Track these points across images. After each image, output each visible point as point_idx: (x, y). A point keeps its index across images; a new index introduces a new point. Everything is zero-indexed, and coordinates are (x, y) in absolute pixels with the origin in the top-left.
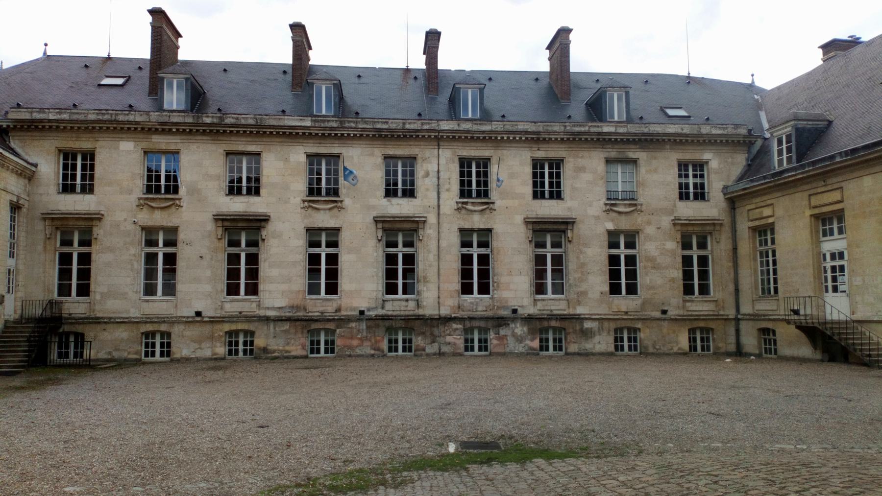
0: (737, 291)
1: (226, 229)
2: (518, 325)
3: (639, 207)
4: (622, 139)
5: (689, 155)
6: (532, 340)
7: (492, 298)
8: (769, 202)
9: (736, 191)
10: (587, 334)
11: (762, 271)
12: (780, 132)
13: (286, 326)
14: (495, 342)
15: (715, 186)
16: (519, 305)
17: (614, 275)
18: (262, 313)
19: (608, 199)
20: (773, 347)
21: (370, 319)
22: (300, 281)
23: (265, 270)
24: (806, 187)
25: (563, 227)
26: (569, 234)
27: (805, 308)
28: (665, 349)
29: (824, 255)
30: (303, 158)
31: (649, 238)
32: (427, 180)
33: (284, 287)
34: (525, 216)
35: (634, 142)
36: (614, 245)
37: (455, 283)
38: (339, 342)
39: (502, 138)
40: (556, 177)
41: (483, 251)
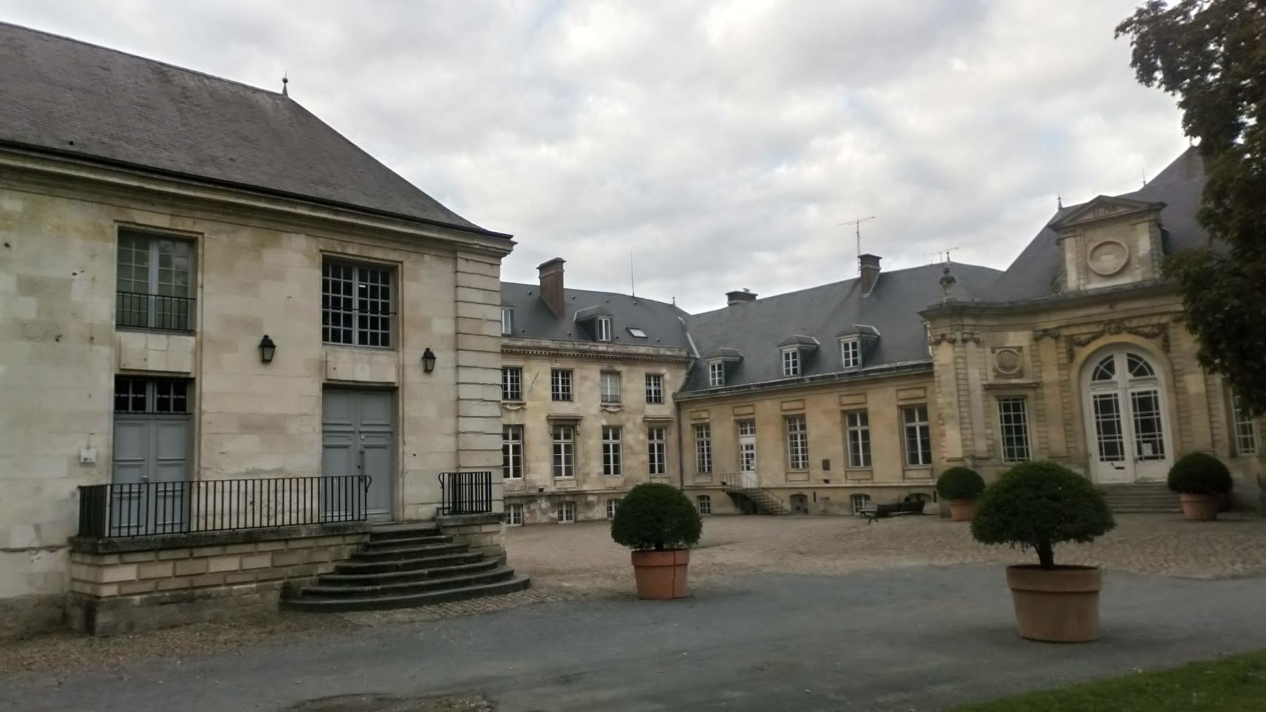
2: (543, 501)
3: (623, 408)
4: (612, 357)
5: (653, 370)
6: (553, 513)
7: (524, 480)
8: (707, 408)
9: (683, 398)
10: (590, 506)
11: (699, 456)
12: (714, 362)
14: (527, 515)
16: (544, 484)
17: (607, 459)
19: (602, 401)
20: (707, 508)
24: (731, 401)
25: (573, 423)
26: (578, 428)
27: (731, 481)
29: (742, 447)
34: (547, 415)
35: (619, 359)
36: (606, 437)
39: (533, 352)
40: (566, 382)
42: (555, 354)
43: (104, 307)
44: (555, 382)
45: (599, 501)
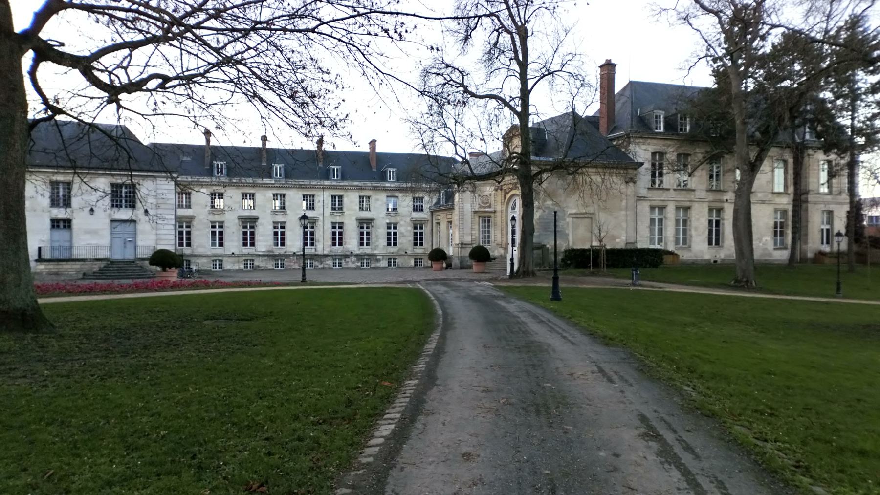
1: (243, 222)
10: (378, 261)
13: (266, 258)
15: (426, 207)
17: (389, 239)
18: (257, 253)
21: (297, 255)
22: (271, 241)
23: (258, 237)
28: (406, 266)
30: (272, 195)
31: (402, 226)
32: (319, 204)
33: (265, 244)
36: (389, 228)
37: (330, 242)
38: (286, 264)
41: (340, 230)
42: (361, 189)
43: (46, 202)
44: (361, 202)
45: (383, 259)
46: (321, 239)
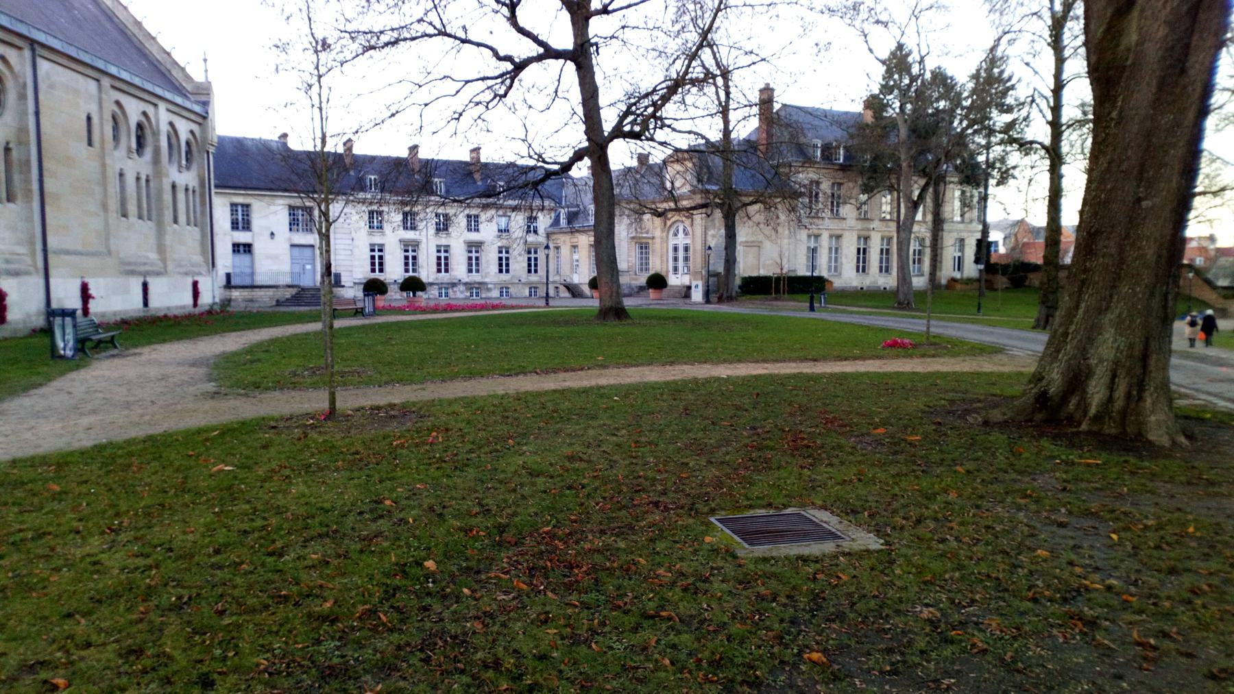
0: (547, 272)
10: (489, 290)
15: (541, 230)
17: (501, 265)
36: (500, 252)
37: (435, 268)
46: (425, 265)
